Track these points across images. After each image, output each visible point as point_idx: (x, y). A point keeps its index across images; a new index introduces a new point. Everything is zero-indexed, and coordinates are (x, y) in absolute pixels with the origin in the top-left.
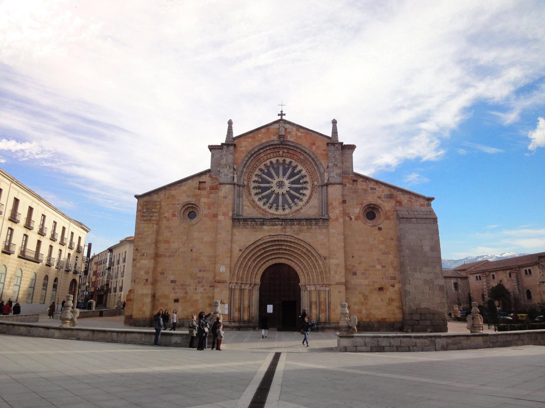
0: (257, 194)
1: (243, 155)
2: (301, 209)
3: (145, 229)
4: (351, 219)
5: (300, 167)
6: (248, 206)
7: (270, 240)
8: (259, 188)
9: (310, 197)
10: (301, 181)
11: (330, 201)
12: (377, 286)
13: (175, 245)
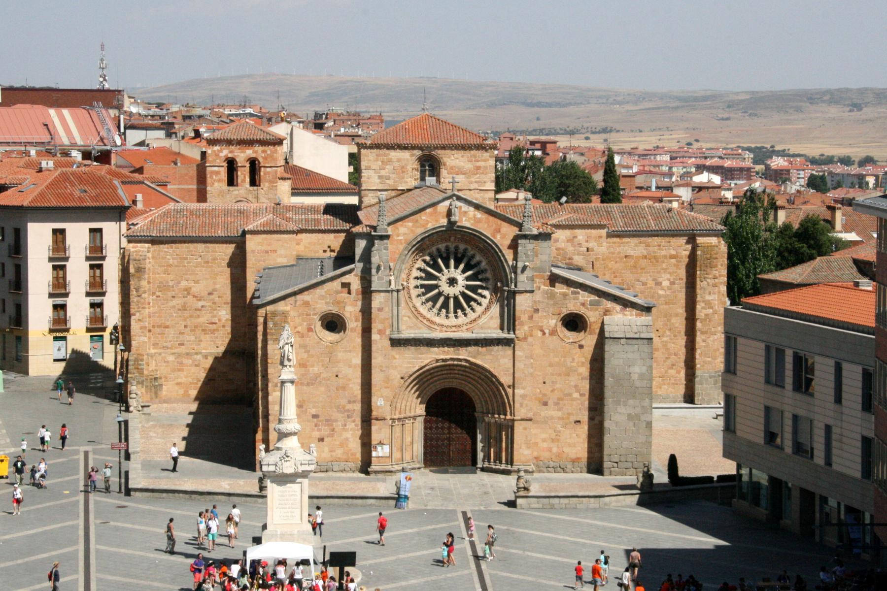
0: (419, 296)
1: (401, 247)
2: (479, 317)
4: (544, 334)
5: (478, 258)
8: (422, 286)
10: (480, 277)
11: (517, 314)
13: (315, 369)
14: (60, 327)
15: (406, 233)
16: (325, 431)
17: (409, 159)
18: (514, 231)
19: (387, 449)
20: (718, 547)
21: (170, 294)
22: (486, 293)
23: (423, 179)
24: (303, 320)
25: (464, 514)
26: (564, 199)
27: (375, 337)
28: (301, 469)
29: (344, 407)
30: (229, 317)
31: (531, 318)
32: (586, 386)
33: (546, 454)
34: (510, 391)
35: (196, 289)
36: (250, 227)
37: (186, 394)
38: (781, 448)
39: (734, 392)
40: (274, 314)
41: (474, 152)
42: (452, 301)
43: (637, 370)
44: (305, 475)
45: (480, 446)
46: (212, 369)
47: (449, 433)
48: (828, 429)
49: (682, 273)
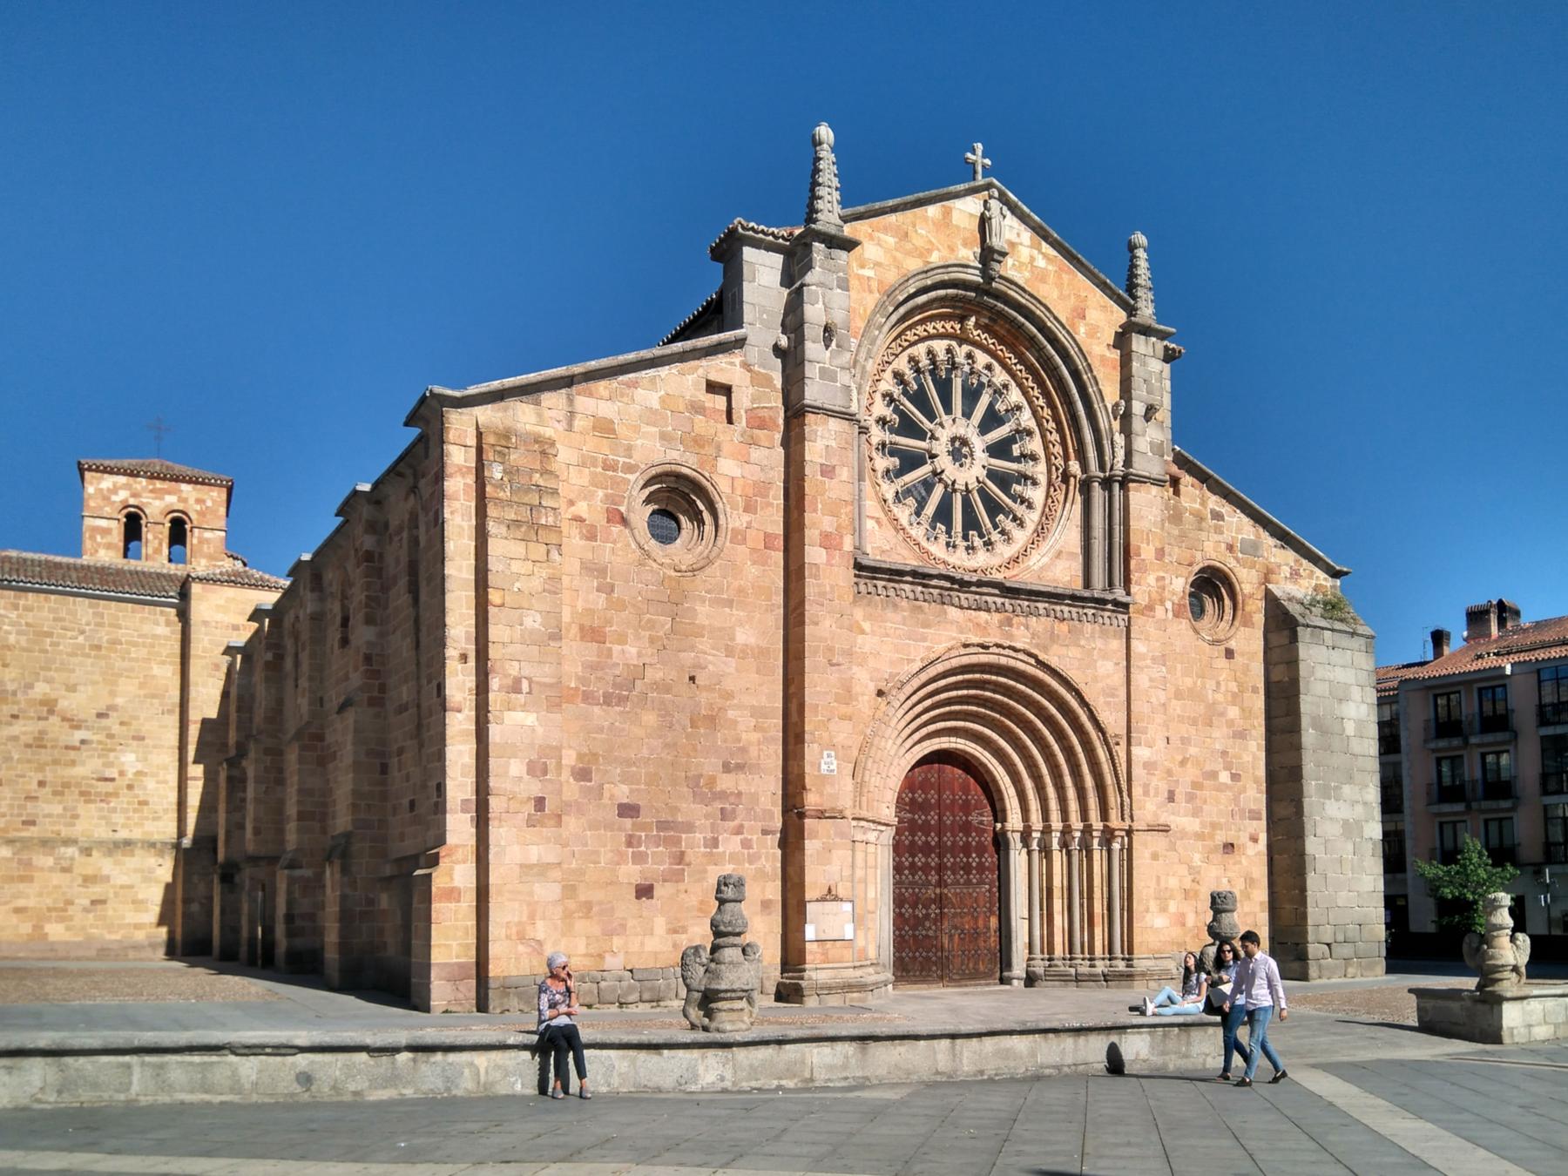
2: (1025, 552)
3: (516, 567)
6: (878, 521)
7: (965, 660)
9: (1047, 515)
11: (1134, 540)
13: (629, 652)
16: (657, 863)
24: (595, 483)
27: (814, 554)
29: (712, 781)
42: (958, 502)
47: (940, 883)
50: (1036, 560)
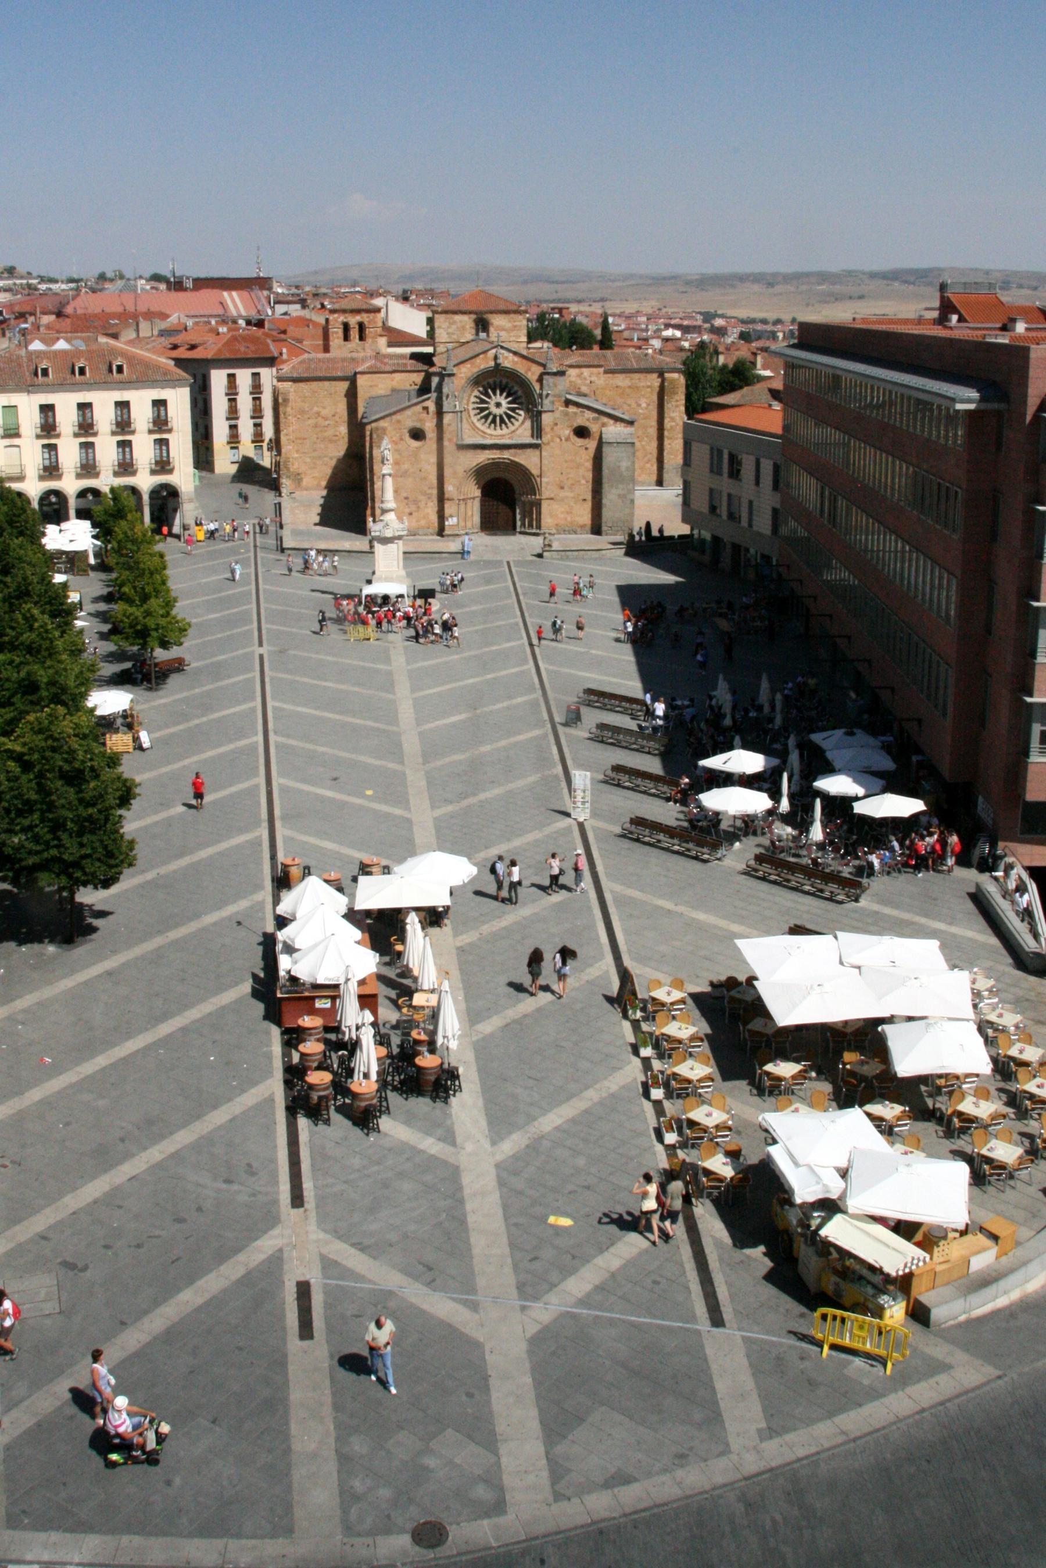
1: (463, 382)
5: (516, 388)
8: (478, 408)
12: (581, 498)
13: (406, 466)
14: (234, 439)
15: (466, 372)
16: (413, 508)
17: (467, 321)
18: (540, 370)
19: (455, 520)
20: (677, 583)
21: (306, 416)
22: (522, 412)
23: (477, 334)
25: (508, 563)
26: (574, 347)
27: (446, 443)
28: (397, 534)
30: (346, 431)
31: (552, 429)
32: (590, 475)
33: (562, 522)
34: (538, 479)
35: (324, 412)
36: (359, 369)
37: (319, 485)
38: (720, 516)
39: (689, 479)
40: (377, 429)
41: (512, 316)
43: (624, 464)
44: (400, 538)
45: (518, 517)
46: (336, 468)
48: (751, 503)
49: (655, 398)
50: (520, 431)
